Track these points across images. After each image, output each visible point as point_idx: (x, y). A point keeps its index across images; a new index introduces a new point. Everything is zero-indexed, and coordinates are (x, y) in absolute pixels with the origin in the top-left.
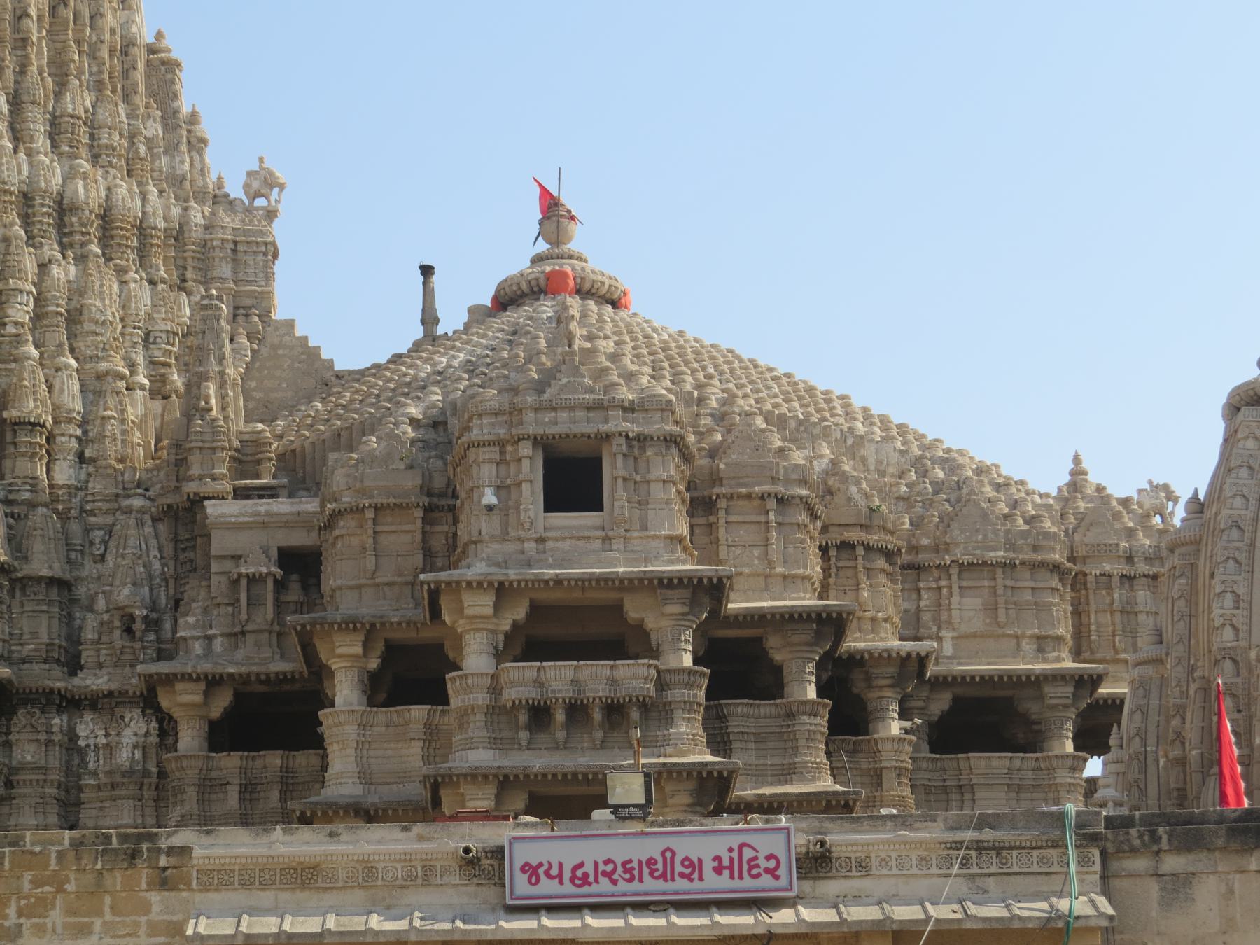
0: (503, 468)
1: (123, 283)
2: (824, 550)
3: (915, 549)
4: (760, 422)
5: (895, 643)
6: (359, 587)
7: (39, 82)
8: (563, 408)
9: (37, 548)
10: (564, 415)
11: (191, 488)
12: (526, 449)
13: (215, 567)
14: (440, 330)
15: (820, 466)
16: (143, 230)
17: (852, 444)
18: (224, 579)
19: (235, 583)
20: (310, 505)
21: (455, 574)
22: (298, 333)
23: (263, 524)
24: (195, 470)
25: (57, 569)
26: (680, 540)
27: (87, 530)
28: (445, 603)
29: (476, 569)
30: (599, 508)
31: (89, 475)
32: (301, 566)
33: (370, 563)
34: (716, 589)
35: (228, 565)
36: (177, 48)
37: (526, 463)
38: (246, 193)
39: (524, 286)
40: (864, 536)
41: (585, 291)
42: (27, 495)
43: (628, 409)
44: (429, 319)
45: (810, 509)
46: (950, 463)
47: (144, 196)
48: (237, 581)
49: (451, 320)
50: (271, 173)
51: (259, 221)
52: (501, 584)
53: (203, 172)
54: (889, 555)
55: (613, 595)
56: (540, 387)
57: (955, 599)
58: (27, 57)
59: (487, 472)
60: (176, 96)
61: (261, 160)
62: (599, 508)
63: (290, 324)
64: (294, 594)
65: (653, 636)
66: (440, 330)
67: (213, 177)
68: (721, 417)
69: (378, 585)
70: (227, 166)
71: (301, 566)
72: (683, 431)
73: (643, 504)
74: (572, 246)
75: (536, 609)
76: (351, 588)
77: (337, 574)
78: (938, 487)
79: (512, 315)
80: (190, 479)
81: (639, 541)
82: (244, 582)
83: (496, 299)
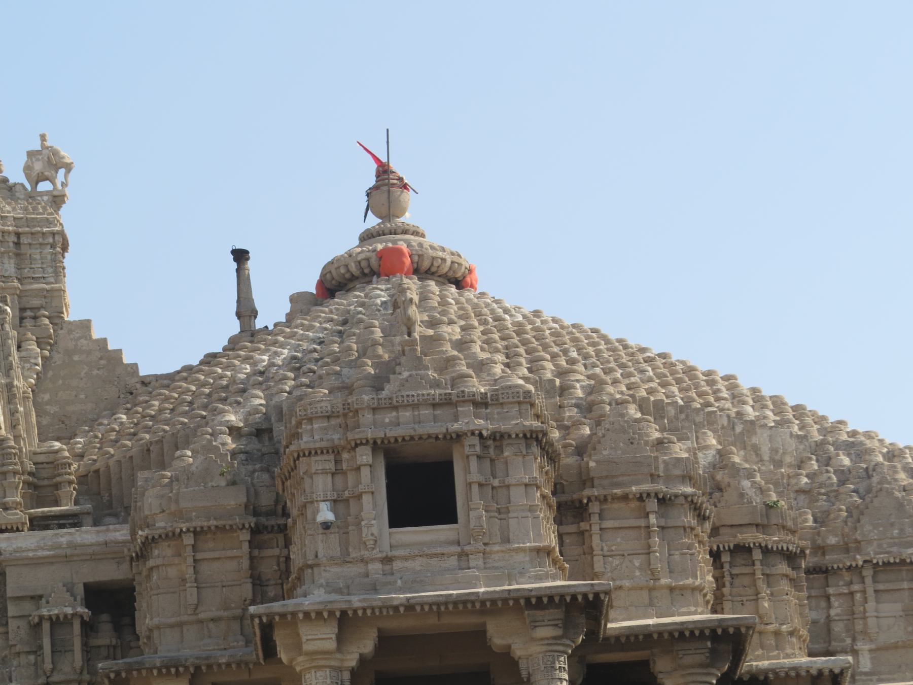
0: (339, 479)
2: (716, 555)
3: (820, 550)
4: (633, 412)
5: (804, 660)
6: (180, 625)
10: (406, 414)
12: (364, 456)
13: (12, 610)
14: (259, 324)
15: (705, 459)
17: (740, 431)
18: (23, 623)
19: (36, 627)
20: (119, 533)
21: (290, 604)
22: (96, 334)
23: (66, 558)
26: (549, 552)
28: (280, 638)
30: (453, 519)
32: (112, 603)
33: (191, 595)
34: (589, 608)
35: (27, 607)
37: (365, 472)
38: (28, 177)
39: (353, 268)
40: (760, 538)
41: (427, 269)
43: (480, 403)
44: (246, 310)
45: (697, 509)
46: (856, 446)
48: (39, 625)
49: (271, 311)
50: (55, 153)
51: (44, 208)
52: (344, 613)
54: (791, 558)
55: (474, 620)
56: (378, 383)
57: (871, 605)
59: (322, 485)
61: (43, 138)
62: (453, 519)
63: (85, 325)
64: (105, 637)
65: (523, 665)
66: (259, 324)
68: (587, 408)
69: (201, 622)
71: (112, 603)
72: (544, 426)
73: (503, 512)
74: (408, 218)
75: (385, 641)
76: (172, 626)
77: (154, 611)
78: (844, 476)
79: (341, 302)
81: (501, 556)
82: (46, 626)
83: (321, 284)
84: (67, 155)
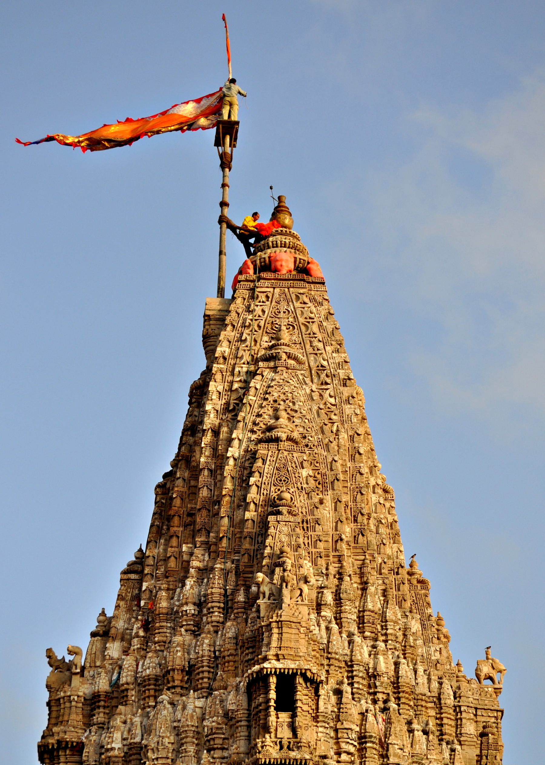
1: (411, 731)
47: (415, 671)
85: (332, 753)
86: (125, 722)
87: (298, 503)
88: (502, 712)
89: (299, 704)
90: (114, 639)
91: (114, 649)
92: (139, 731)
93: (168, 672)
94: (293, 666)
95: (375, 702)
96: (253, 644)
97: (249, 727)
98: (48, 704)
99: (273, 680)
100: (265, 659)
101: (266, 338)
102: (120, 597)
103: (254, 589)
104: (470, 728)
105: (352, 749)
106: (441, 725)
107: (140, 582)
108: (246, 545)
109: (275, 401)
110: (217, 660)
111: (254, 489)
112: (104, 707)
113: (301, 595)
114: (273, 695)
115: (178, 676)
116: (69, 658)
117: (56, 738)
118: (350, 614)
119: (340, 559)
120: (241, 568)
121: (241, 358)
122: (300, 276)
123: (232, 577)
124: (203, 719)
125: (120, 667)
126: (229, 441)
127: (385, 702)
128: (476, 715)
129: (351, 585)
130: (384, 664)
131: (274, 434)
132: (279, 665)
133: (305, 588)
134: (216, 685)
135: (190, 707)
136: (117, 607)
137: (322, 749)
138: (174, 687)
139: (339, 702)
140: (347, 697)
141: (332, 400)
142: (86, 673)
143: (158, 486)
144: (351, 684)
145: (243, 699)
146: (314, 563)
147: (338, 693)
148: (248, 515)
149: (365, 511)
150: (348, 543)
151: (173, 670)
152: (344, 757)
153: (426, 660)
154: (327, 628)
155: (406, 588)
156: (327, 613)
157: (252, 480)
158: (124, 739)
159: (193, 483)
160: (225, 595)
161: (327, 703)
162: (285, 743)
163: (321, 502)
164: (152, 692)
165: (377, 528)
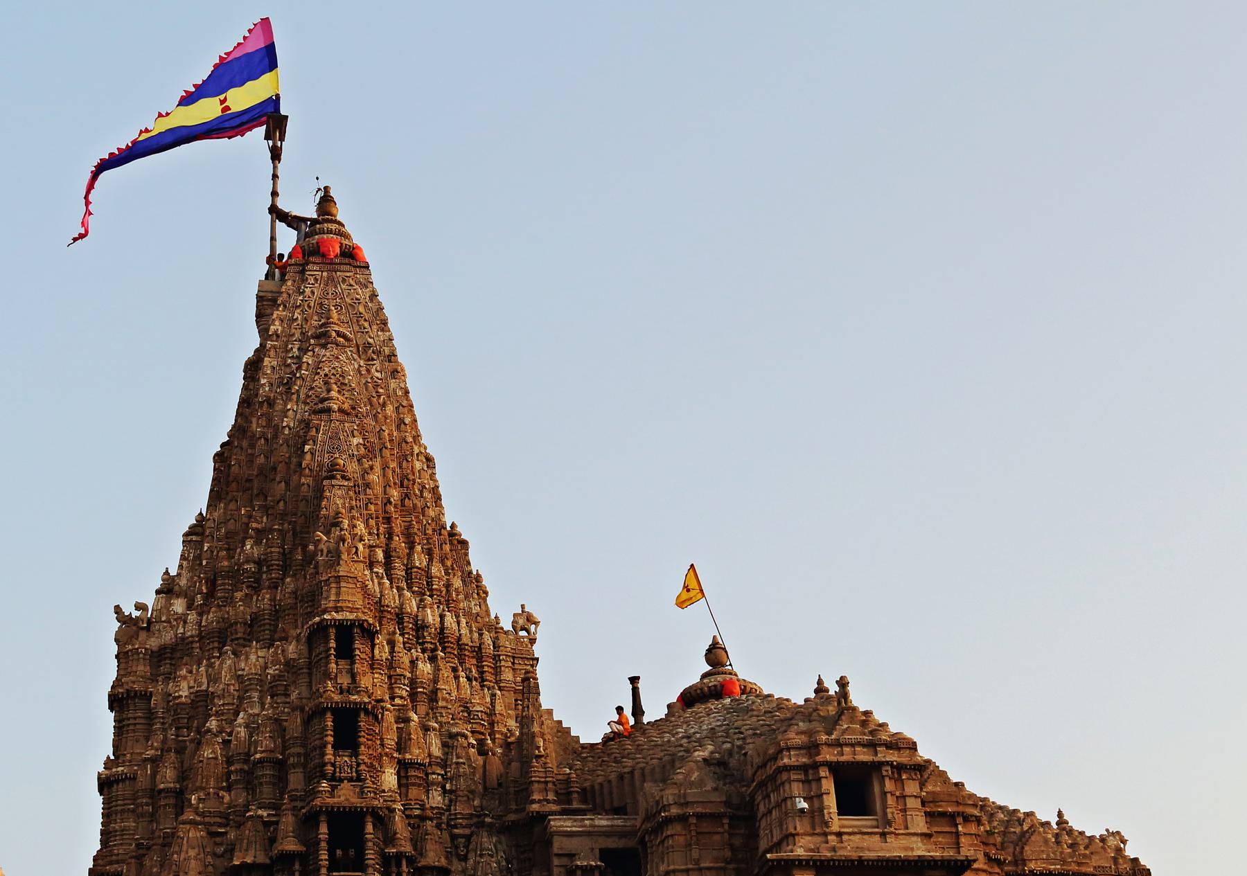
6: (687, 871)
7: (399, 543)
8: (846, 745)
9: (430, 846)
10: (847, 749)
11: (535, 807)
12: (824, 772)
13: (556, 861)
14: (646, 719)
16: (461, 646)
18: (562, 870)
23: (588, 834)
24: (536, 797)
25: (443, 862)
27: (454, 837)
29: (800, 852)
31: (451, 801)
35: (565, 861)
36: (465, 533)
42: (417, 812)
44: (638, 711)
47: (458, 623)
49: (654, 711)
53: (488, 612)
58: (391, 528)
60: (469, 563)
61: (523, 607)
63: (550, 712)
67: (493, 616)
69: (700, 869)
70: (502, 609)
76: (682, 871)
79: (700, 708)
80: (533, 802)
84: (537, 615)
85: (387, 697)
86: (191, 672)
87: (349, 469)
88: (537, 659)
89: (357, 652)
90: (178, 596)
91: (179, 606)
92: (205, 680)
93: (231, 625)
94: (352, 616)
95: (424, 651)
96: (311, 599)
97: (310, 674)
98: (117, 657)
99: (332, 632)
100: (325, 611)
101: (316, 318)
102: (183, 557)
103: (311, 547)
104: (508, 675)
105: (404, 694)
106: (483, 672)
107: (201, 543)
108: (302, 506)
109: (326, 375)
110: (277, 613)
111: (308, 457)
112: (171, 659)
113: (356, 553)
114: (333, 644)
115: (240, 628)
116: (136, 614)
117: (126, 687)
118: (400, 572)
119: (388, 520)
120: (298, 529)
121: (293, 335)
122: (347, 261)
123: (289, 536)
124: (266, 668)
125: (185, 622)
126: (285, 413)
127: (434, 650)
128: (513, 663)
129: (399, 543)
130: (431, 617)
131: (326, 404)
132: (338, 616)
133: (361, 547)
134: (276, 636)
135: (253, 657)
136: (181, 566)
137: (378, 693)
138: (237, 639)
139: (392, 651)
140: (399, 647)
141: (378, 375)
142: (152, 628)
143: (217, 455)
144: (402, 635)
145: (304, 648)
146: (367, 525)
147: (392, 643)
148: (303, 480)
149: (411, 477)
150: (395, 506)
151: (236, 623)
152: (397, 701)
153: (468, 614)
154: (379, 584)
155: (447, 547)
156: (381, 571)
157: (307, 447)
158: (190, 688)
159: (250, 451)
160: (284, 554)
161: (382, 652)
162: (345, 686)
163: (371, 468)
164: (216, 645)
165: (421, 492)
